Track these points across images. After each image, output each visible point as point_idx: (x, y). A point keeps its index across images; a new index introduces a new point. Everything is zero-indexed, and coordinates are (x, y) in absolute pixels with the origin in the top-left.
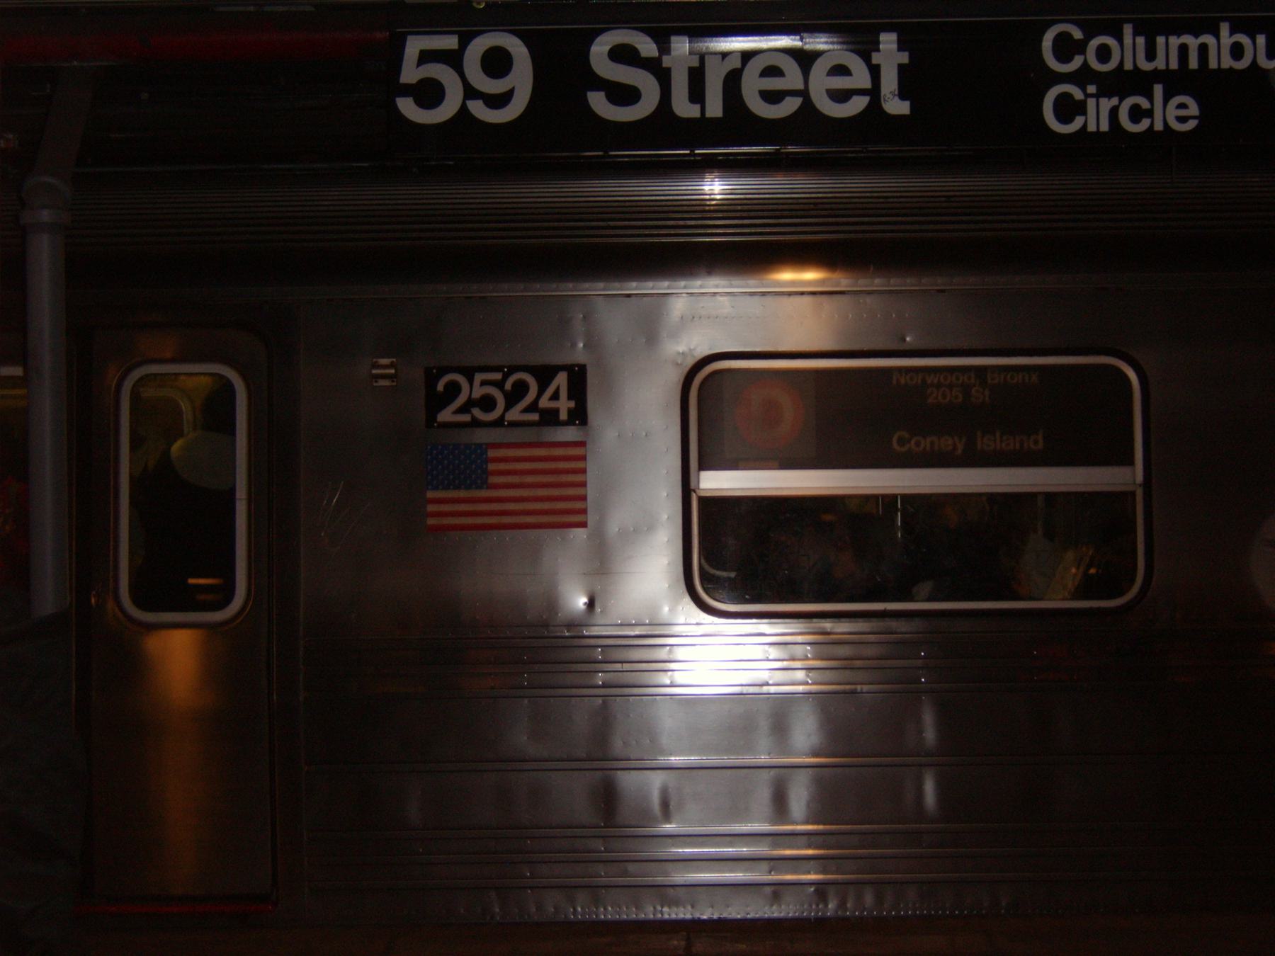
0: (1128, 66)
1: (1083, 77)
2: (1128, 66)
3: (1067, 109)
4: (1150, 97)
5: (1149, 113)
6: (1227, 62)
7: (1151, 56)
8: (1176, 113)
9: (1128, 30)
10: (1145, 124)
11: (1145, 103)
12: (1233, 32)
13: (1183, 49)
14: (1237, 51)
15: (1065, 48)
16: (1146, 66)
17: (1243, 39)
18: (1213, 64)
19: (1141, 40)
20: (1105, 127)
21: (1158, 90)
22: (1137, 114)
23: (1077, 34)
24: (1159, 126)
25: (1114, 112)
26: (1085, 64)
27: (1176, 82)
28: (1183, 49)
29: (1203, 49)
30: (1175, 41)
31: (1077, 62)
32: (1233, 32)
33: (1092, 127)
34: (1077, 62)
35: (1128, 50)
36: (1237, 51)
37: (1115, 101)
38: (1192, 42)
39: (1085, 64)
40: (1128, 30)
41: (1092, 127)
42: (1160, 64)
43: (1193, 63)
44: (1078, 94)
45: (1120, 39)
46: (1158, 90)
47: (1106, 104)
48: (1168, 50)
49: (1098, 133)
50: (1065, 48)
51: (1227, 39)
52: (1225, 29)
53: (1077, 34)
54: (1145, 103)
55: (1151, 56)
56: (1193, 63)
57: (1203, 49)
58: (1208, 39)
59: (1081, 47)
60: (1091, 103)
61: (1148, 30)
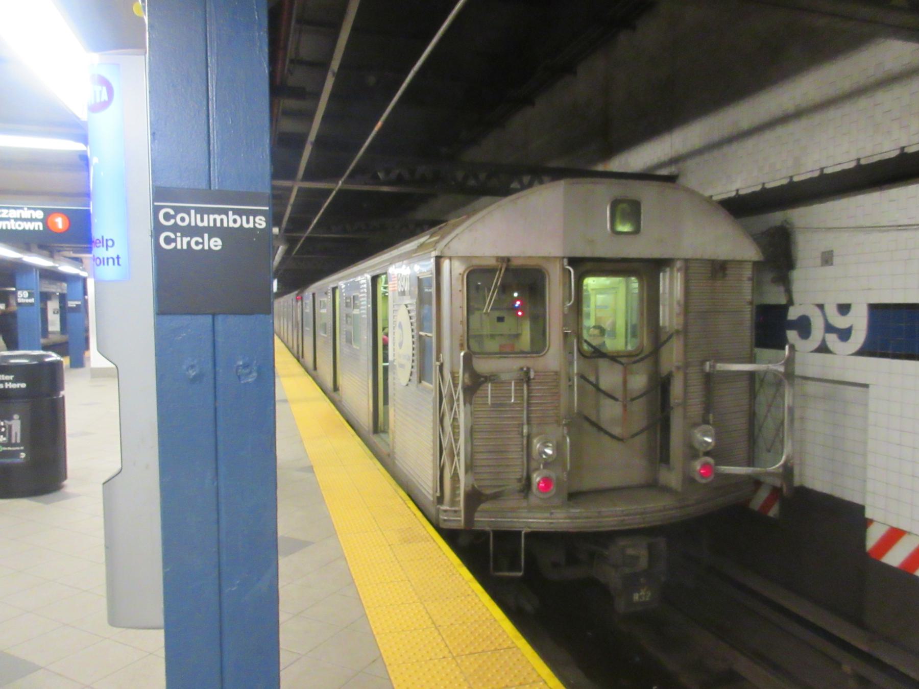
0: (193, 224)
1: (175, 228)
2: (193, 224)
3: (168, 240)
4: (203, 238)
5: (203, 243)
6: (231, 225)
8: (216, 244)
10: (200, 247)
11: (200, 240)
12: (234, 214)
13: (215, 220)
15: (167, 217)
16: (200, 224)
18: (225, 225)
19: (198, 216)
20: (185, 247)
21: (206, 236)
22: (197, 243)
23: (172, 212)
24: (206, 248)
25: (189, 243)
26: (176, 223)
27: (213, 231)
28: (215, 220)
29: (222, 220)
30: (212, 217)
31: (172, 222)
32: (234, 214)
33: (179, 247)
34: (172, 222)
35: (194, 219)
36: (235, 221)
37: (189, 239)
38: (218, 218)
39: (176, 223)
41: (179, 247)
42: (205, 224)
43: (218, 224)
44: (172, 236)
45: (189, 215)
46: (206, 236)
47: (186, 240)
49: (182, 249)
52: (230, 213)
53: (172, 212)
54: (200, 240)
56: (218, 224)
57: (222, 220)
58: (224, 217)
59: (174, 217)
60: (179, 239)
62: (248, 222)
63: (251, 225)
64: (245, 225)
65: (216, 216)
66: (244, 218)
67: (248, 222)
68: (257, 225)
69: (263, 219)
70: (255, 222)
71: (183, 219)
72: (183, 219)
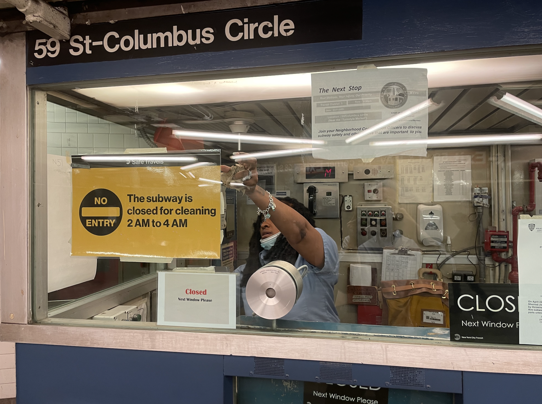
0: (137, 48)
2: (137, 48)
7: (145, 43)
9: (136, 32)
13: (158, 39)
14: (180, 38)
16: (143, 47)
17: (182, 32)
18: (170, 45)
19: (142, 36)
23: (117, 36)
28: (158, 39)
29: (166, 38)
30: (155, 36)
34: (117, 47)
36: (180, 38)
38: (162, 35)
40: (136, 32)
43: (162, 45)
48: (153, 38)
50: (112, 42)
51: (176, 33)
52: (175, 28)
53: (117, 36)
55: (145, 43)
56: (162, 45)
57: (166, 38)
58: (168, 34)
59: (118, 41)
61: (144, 32)
62: (194, 38)
63: (198, 41)
64: (191, 42)
65: (160, 34)
66: (190, 32)
67: (194, 38)
68: (204, 40)
69: (211, 30)
70: (202, 37)
71: (127, 43)
72: (127, 43)
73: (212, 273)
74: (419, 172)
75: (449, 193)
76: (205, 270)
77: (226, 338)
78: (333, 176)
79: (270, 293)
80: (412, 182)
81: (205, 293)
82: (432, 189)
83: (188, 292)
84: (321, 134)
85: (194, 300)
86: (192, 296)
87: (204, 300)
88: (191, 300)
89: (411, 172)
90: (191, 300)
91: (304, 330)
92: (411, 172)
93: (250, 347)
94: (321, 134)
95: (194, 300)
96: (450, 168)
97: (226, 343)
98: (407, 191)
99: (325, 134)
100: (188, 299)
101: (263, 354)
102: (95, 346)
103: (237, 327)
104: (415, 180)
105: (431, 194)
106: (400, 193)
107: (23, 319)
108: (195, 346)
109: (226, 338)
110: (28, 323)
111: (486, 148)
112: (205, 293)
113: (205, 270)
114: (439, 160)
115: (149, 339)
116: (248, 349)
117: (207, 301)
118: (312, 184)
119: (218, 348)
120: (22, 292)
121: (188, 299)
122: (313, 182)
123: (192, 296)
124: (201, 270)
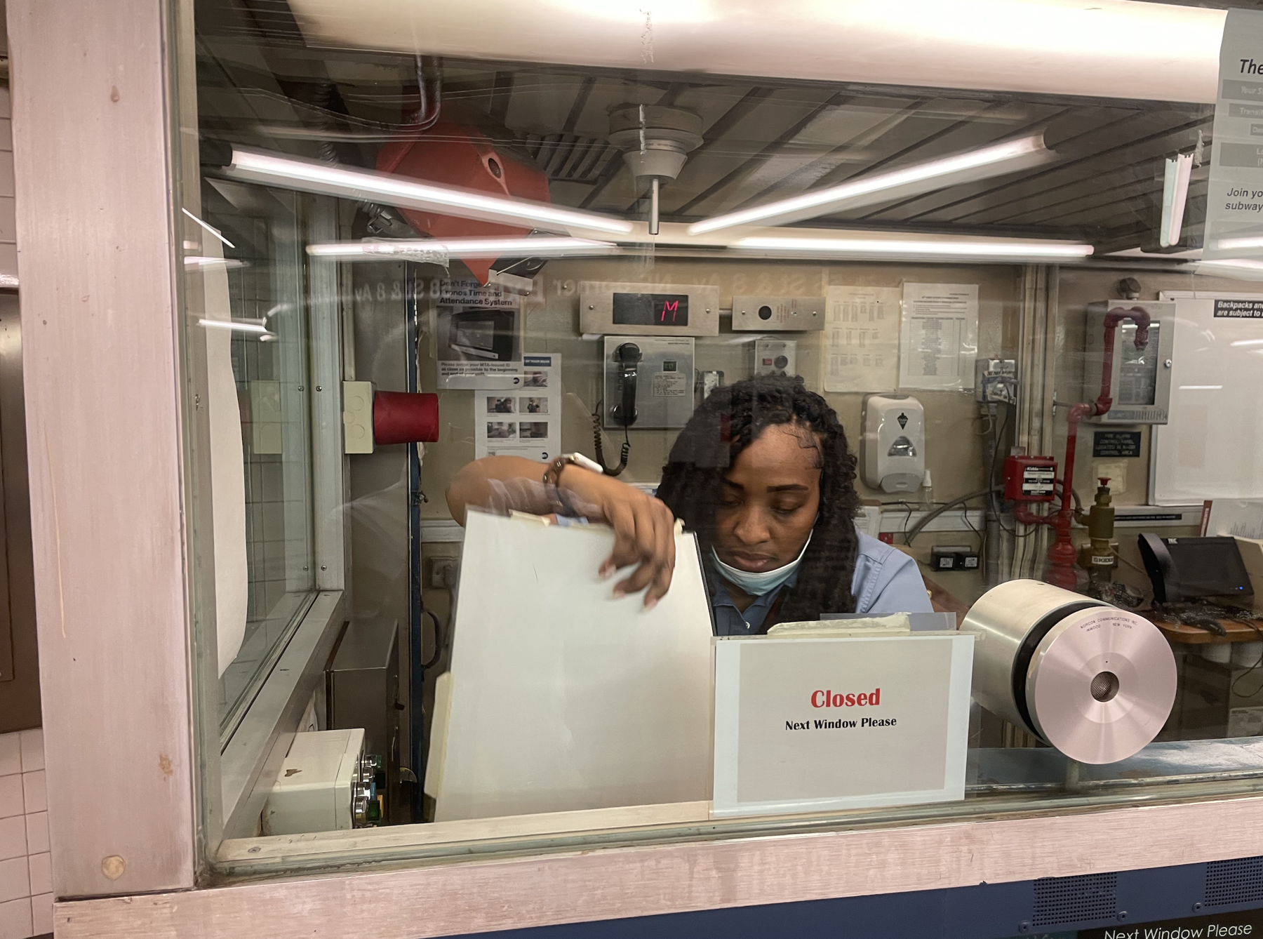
73: (898, 634)
74: (871, 319)
75: (930, 370)
76: (877, 625)
77: (969, 836)
78: (683, 321)
79: (1107, 686)
80: (855, 341)
81: (874, 698)
82: (895, 360)
83: (820, 699)
84: (1234, 200)
85: (839, 724)
86: (832, 714)
87: (872, 723)
88: (831, 725)
89: (855, 318)
90: (831, 725)
91: (1148, 780)
92: (855, 318)
93: (1038, 851)
94: (1234, 200)
95: (839, 724)
96: (936, 313)
97: (970, 851)
98: (844, 363)
99: (1246, 200)
100: (818, 724)
101: (1074, 866)
102: (508, 925)
103: (967, 795)
104: (862, 336)
105: (895, 372)
106: (829, 368)
107: (172, 868)
108: (871, 872)
109: (969, 836)
110: (196, 883)
111: (1011, 271)
112: (874, 698)
113: (877, 625)
114: (914, 291)
115: (714, 873)
116: (1034, 858)
117: (882, 724)
118: (627, 340)
119: (943, 869)
120: (165, 765)
121: (818, 724)
122: (630, 335)
123: (832, 714)
124: (865, 626)
